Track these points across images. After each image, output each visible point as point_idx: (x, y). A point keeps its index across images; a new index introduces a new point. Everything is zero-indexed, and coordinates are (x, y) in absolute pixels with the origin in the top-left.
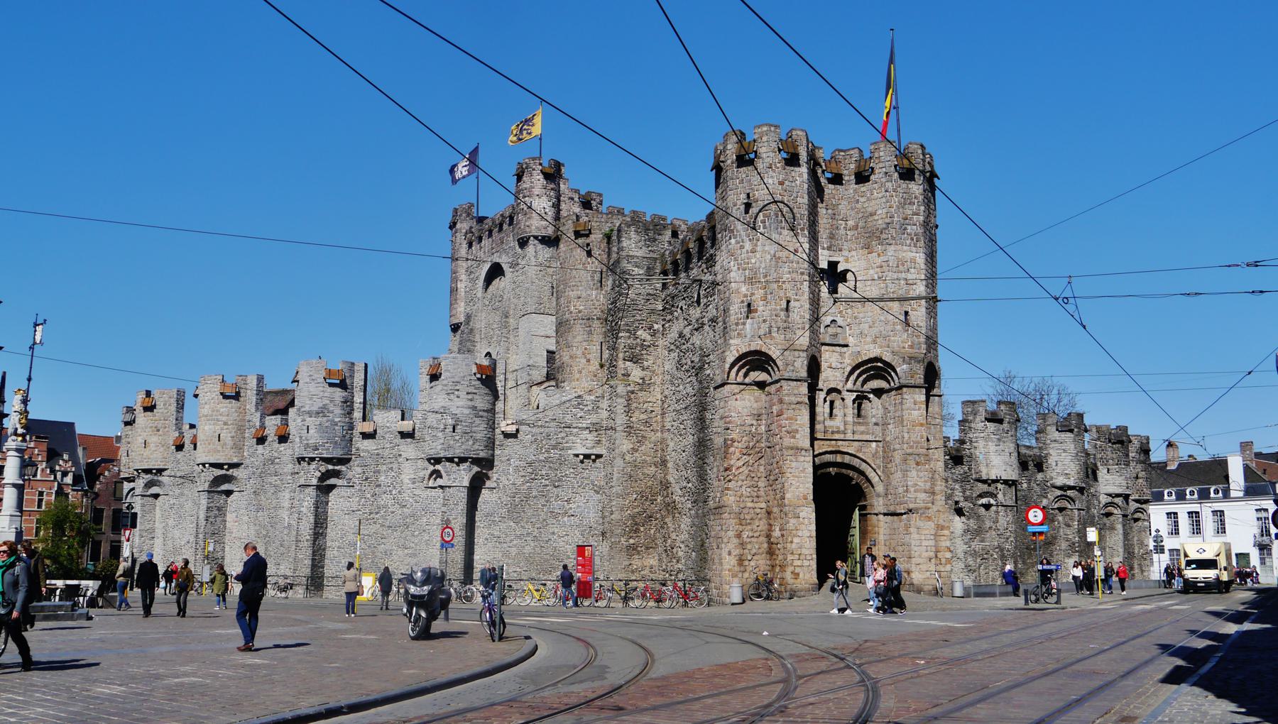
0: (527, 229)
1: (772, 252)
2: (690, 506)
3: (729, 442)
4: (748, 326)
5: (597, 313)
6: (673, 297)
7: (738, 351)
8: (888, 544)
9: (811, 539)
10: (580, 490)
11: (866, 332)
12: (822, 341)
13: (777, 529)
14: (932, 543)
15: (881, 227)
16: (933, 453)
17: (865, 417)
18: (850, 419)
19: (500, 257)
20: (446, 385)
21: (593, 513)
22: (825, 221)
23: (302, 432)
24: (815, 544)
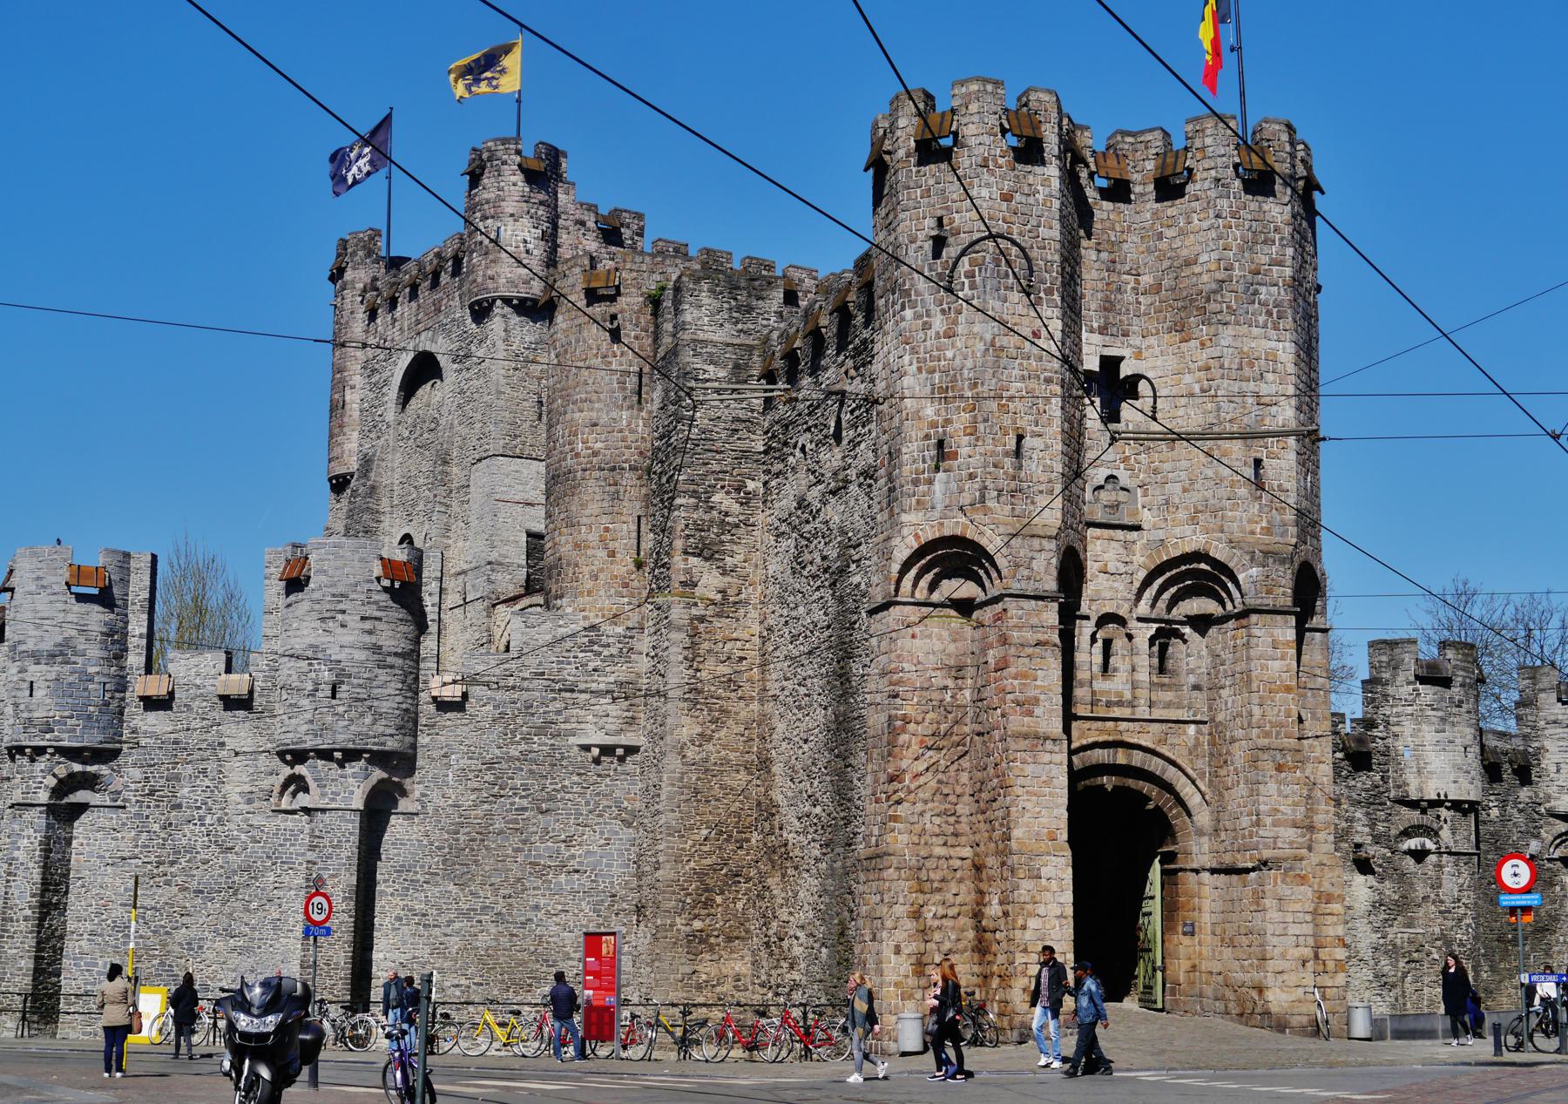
0: (490, 284)
1: (988, 337)
2: (817, 853)
3: (899, 723)
4: (938, 487)
5: (631, 456)
6: (786, 426)
7: (917, 536)
8: (1218, 931)
9: (1064, 922)
10: (593, 819)
11: (1177, 500)
12: (1088, 518)
13: (995, 901)
14: (1308, 929)
15: (1206, 288)
16: (1311, 746)
17: (1174, 673)
18: (1143, 676)
19: (433, 340)
20: (318, 602)
21: (620, 866)
22: (1095, 274)
23: (19, 694)
24: (1072, 931)
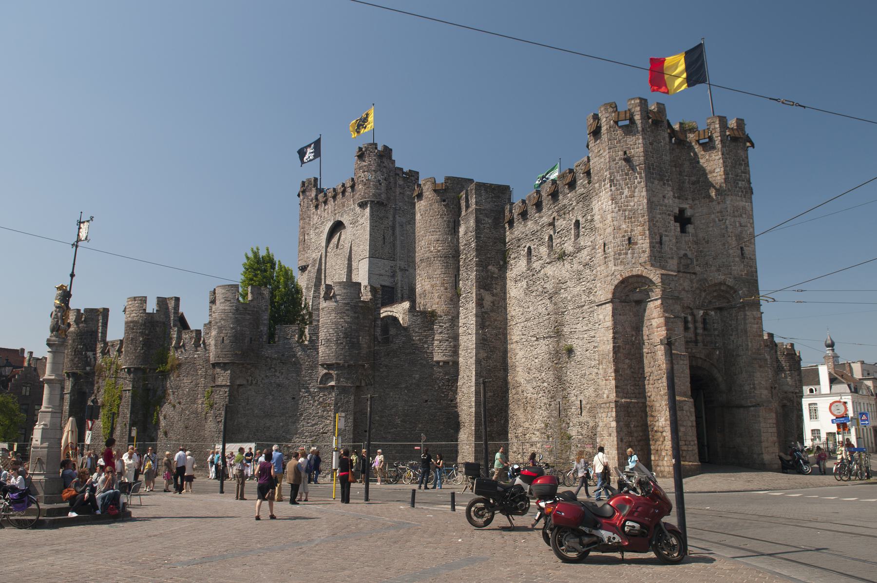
4: (629, 256)
6: (519, 240)
9: (693, 428)
18: (700, 331)
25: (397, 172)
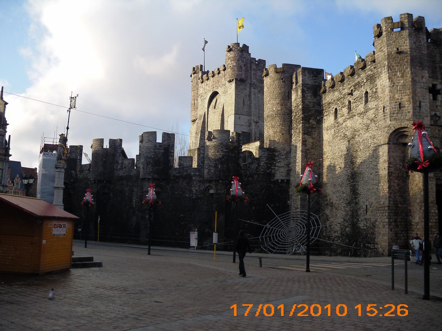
2: (344, 205)
6: (330, 103)
25: (252, 61)
